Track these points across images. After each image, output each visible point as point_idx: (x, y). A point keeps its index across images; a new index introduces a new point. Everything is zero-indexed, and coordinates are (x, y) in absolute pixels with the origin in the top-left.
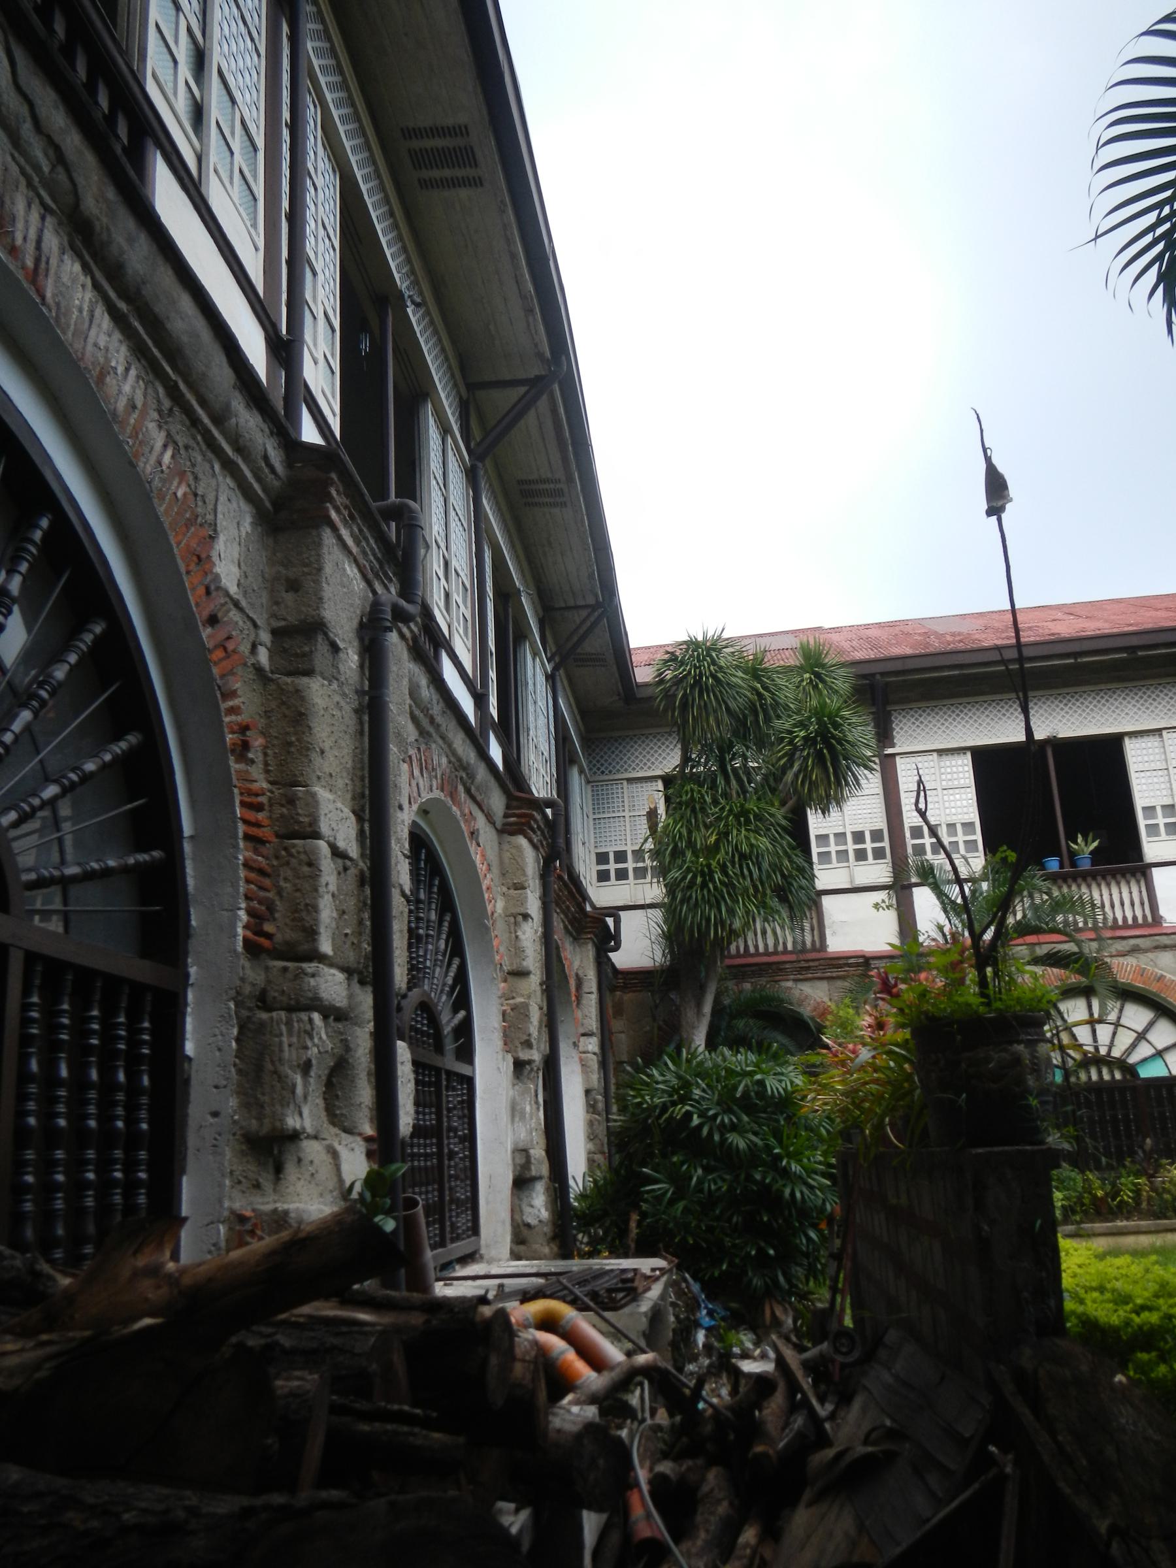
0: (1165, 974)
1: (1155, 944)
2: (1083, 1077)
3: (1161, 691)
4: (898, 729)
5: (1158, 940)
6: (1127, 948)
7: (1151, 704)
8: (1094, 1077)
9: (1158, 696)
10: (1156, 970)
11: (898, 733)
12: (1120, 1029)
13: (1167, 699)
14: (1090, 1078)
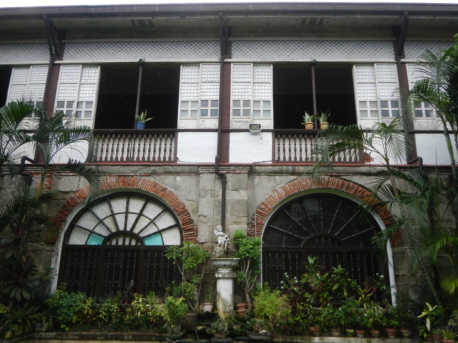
0: (167, 187)
1: (165, 170)
2: (114, 243)
3: (205, 45)
4: (66, 52)
5: (166, 169)
6: (150, 172)
7: (198, 50)
9: (202, 47)
10: (163, 185)
11: (66, 54)
12: (142, 217)
13: (207, 48)
14: (117, 243)
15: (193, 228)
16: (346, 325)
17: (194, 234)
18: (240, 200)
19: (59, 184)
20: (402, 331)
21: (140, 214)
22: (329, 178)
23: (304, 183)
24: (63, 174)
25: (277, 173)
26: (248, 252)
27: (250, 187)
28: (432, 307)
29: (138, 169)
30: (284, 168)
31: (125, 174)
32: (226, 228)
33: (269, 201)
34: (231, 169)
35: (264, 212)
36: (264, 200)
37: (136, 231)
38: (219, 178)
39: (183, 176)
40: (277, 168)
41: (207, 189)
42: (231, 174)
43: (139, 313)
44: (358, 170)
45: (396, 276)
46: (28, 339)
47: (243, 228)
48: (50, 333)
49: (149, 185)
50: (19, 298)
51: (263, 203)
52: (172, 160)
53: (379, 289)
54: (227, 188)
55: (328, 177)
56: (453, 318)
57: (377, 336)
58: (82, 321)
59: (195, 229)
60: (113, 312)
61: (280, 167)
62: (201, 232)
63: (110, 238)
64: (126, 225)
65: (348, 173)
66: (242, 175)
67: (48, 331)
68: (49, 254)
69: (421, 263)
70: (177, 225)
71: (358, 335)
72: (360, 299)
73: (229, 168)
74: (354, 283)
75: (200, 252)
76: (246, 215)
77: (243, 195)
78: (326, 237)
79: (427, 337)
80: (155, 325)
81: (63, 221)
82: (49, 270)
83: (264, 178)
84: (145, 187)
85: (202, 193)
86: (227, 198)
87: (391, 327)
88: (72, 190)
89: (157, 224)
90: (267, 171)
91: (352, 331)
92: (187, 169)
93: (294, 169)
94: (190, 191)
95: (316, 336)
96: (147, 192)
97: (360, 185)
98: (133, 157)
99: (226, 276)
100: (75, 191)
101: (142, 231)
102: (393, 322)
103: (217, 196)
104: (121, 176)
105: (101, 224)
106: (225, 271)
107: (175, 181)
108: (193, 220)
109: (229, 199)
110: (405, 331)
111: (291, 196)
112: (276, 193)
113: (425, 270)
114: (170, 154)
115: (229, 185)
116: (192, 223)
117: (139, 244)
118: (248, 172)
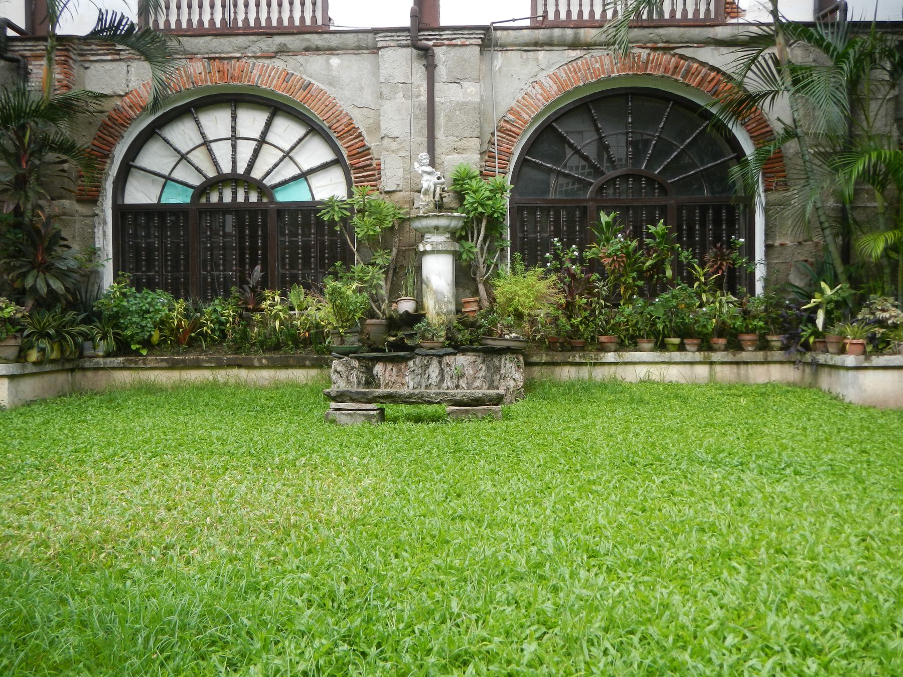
0: (313, 81)
1: (305, 44)
2: (214, 198)
5: (308, 40)
6: (274, 49)
8: (241, 198)
10: (304, 77)
12: (265, 146)
14: (221, 198)
15: (371, 165)
16: (666, 332)
17: (373, 175)
18: (464, 104)
19: (86, 81)
20: (769, 338)
21: (262, 141)
22: (649, 54)
23: (598, 66)
24: (92, 58)
25: (542, 45)
26: (482, 205)
27: (486, 77)
28: (832, 288)
29: (248, 44)
30: (557, 32)
31: (223, 55)
32: (437, 161)
33: (523, 104)
34: (444, 37)
35: (513, 129)
36: (514, 104)
37: (257, 174)
38: (420, 57)
39: (344, 57)
40: (541, 34)
41: (395, 81)
42: (444, 48)
43: (277, 323)
44: (711, 35)
45: (768, 247)
46: (72, 370)
47: (471, 160)
48: (112, 359)
49: (274, 78)
50: (43, 290)
51: (511, 110)
52: (320, 22)
53: (734, 264)
54: (437, 77)
55: (648, 51)
56: (868, 306)
57: (723, 347)
58: (171, 340)
59: (374, 165)
60: (228, 321)
61: (547, 31)
62: (386, 171)
63: (205, 189)
64: (234, 162)
65: (690, 43)
66: (468, 48)
67: (108, 355)
68: (88, 221)
69: (821, 212)
70: (338, 161)
71: (688, 347)
72: (696, 284)
73: (441, 35)
74: (685, 255)
75: (388, 204)
76: (476, 133)
77: (471, 92)
78: (637, 177)
79: (814, 342)
80: (307, 342)
81: (107, 156)
82: (93, 253)
83: (514, 56)
84: (267, 82)
85: (386, 90)
86: (437, 99)
87: (748, 332)
88: (115, 93)
89: (298, 159)
90: (521, 40)
91: (677, 341)
92: (351, 39)
93: (576, 34)
94: (361, 89)
95: (610, 351)
96: (272, 92)
97: (713, 68)
98: (236, 19)
99: (440, 248)
100: (122, 93)
101: (268, 173)
102: (755, 323)
103: (418, 96)
104: (214, 59)
105: (184, 161)
106: (439, 239)
107: (328, 66)
108: (369, 149)
109: (442, 100)
110: (775, 338)
111: (568, 94)
112: (537, 87)
113: (826, 225)
114: (314, 11)
115: (442, 71)
116: (369, 154)
117: (265, 200)
118: (480, 42)
